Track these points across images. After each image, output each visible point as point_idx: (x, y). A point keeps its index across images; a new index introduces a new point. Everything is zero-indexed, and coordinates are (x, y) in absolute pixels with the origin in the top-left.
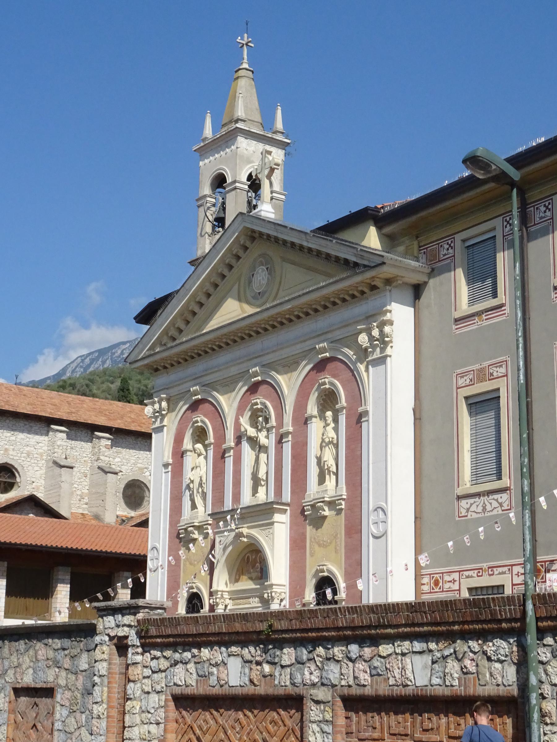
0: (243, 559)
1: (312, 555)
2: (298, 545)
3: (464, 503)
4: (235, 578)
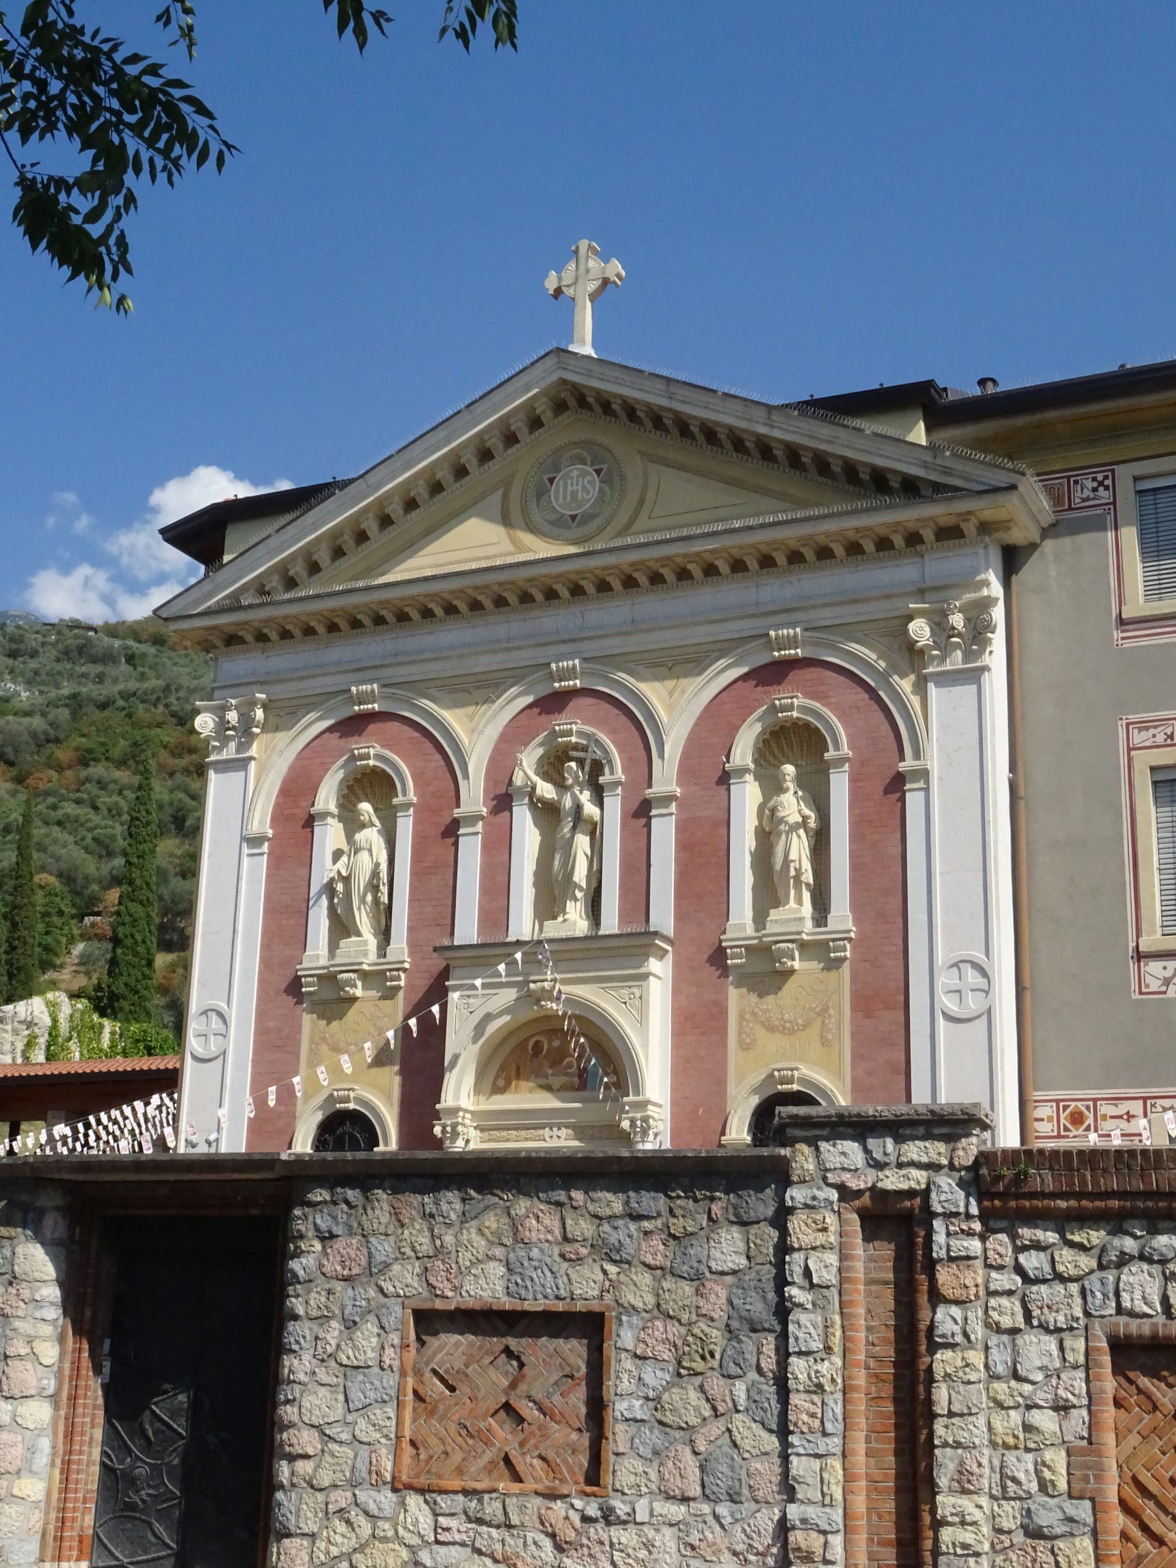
0: (521, 1046)
1: (745, 1047)
2: (699, 1028)
3: (1155, 968)
4: (494, 1084)
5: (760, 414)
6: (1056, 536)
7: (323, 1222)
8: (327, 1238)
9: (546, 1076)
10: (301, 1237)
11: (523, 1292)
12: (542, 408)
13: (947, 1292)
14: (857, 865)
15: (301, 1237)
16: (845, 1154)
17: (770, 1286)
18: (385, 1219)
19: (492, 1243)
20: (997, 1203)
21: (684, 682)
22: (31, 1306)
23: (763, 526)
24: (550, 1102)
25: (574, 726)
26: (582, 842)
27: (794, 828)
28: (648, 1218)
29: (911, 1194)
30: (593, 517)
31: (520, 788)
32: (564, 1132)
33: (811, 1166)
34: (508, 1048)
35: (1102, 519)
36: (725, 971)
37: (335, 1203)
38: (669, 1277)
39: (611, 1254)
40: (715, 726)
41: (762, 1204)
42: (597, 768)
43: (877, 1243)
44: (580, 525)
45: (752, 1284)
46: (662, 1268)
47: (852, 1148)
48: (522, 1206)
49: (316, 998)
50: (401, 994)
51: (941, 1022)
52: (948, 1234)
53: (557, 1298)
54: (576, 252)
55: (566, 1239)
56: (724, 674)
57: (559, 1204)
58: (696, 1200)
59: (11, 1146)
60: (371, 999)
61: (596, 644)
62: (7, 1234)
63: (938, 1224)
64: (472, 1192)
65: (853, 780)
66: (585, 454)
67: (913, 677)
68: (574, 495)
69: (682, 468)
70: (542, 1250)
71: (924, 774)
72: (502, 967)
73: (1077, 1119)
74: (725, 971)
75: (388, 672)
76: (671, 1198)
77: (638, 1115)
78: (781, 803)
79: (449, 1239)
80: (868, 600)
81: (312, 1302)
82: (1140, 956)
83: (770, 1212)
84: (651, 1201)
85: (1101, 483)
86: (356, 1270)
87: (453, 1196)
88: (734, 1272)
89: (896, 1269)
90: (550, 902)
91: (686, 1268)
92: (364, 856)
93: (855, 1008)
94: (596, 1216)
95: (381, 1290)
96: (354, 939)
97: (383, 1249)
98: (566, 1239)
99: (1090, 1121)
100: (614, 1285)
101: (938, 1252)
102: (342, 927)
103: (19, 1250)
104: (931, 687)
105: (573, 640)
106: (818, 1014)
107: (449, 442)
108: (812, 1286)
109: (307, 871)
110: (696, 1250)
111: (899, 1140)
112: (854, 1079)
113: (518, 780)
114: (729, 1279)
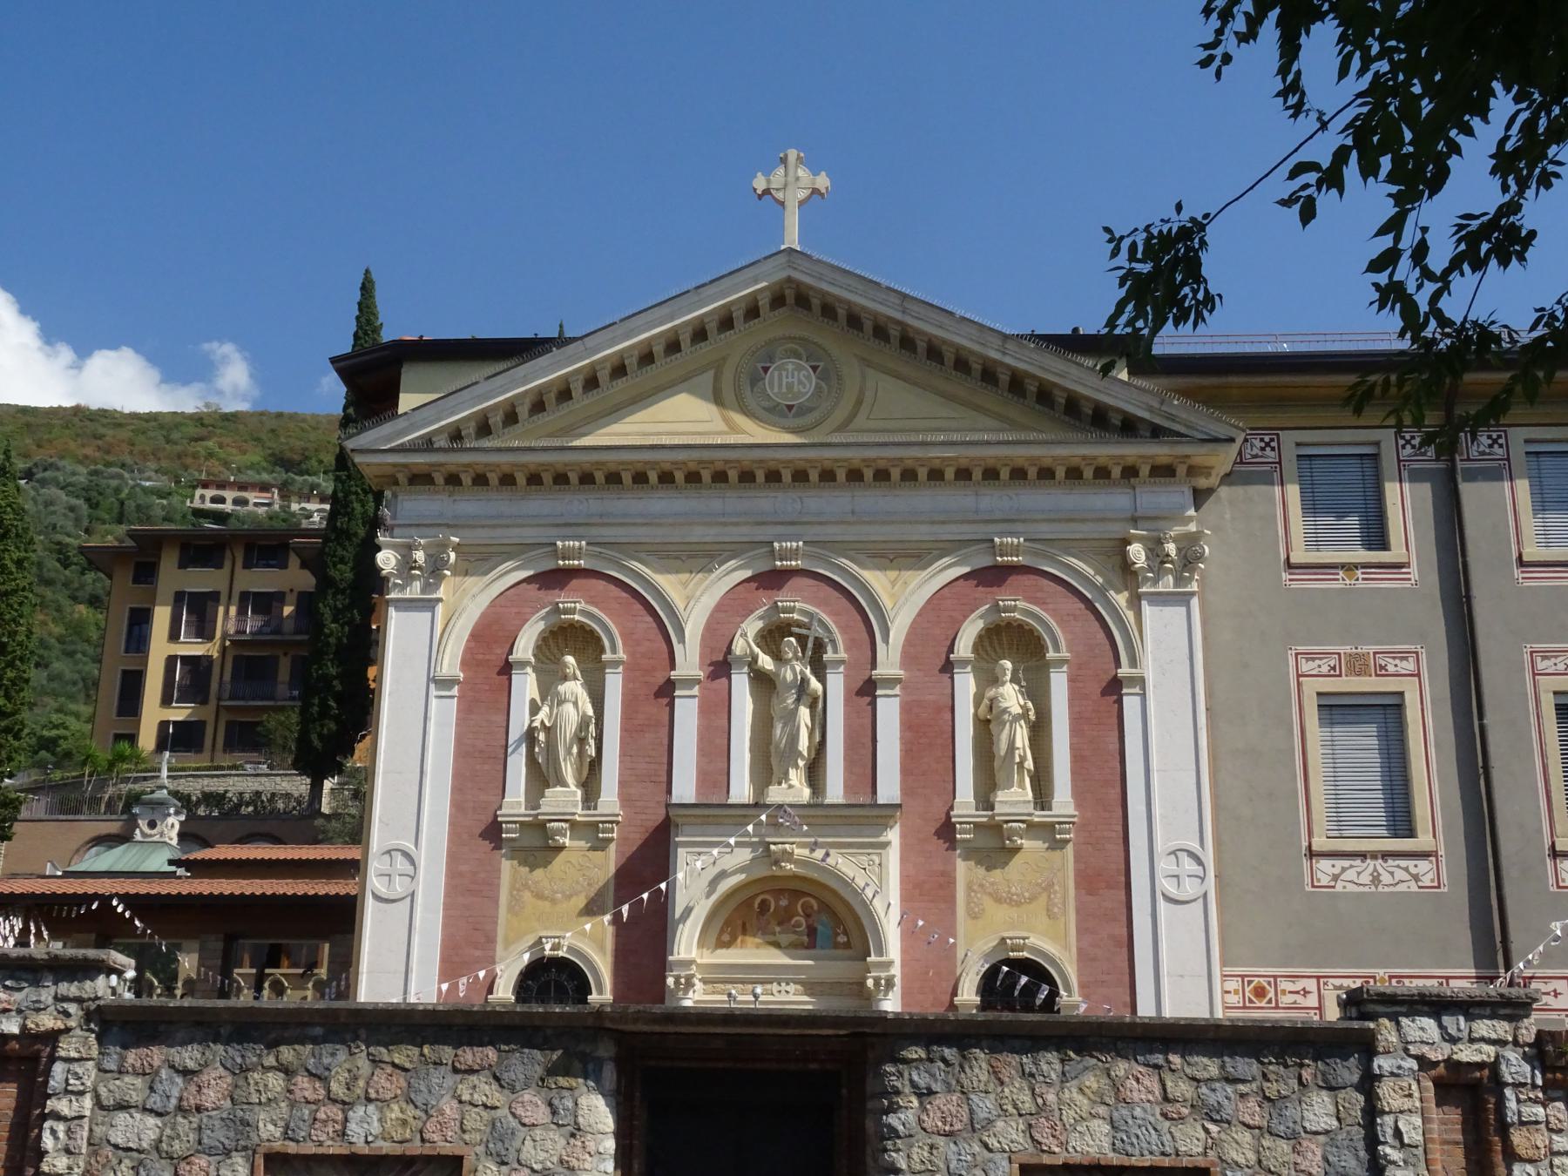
0: (748, 903)
1: (973, 916)
2: (929, 894)
3: (1324, 865)
4: (718, 939)
5: (997, 342)
6: (1231, 484)
7: (922, 1080)
8: (925, 1094)
9: (774, 934)
10: (898, 1093)
11: (1129, 1149)
12: (764, 302)
13: (1522, 1152)
14: (1078, 758)
15: (898, 1093)
16: (1423, 1028)
17: (1361, 1145)
18: (984, 1078)
19: (1094, 1102)
20: (1559, 1075)
21: (907, 574)
22: (595, 1159)
23: (999, 443)
24: (778, 958)
25: (796, 603)
26: (804, 713)
27: (1016, 718)
28: (1243, 1081)
29: (1481, 1066)
30: (811, 410)
31: (739, 658)
32: (792, 988)
33: (1394, 1038)
34: (732, 904)
35: (1271, 475)
36: (952, 843)
37: (931, 1061)
38: (1267, 1136)
39: (1211, 1114)
40: (938, 618)
41: (1348, 1071)
42: (819, 647)
43: (1446, 1108)
44: (797, 415)
45: (1346, 1143)
46: (1259, 1128)
47: (1429, 1023)
48: (1121, 1067)
49: (517, 844)
50: (613, 846)
51: (1162, 905)
52: (1519, 1101)
53: (1163, 1154)
54: (784, 161)
55: (1166, 1099)
56: (946, 571)
57: (1157, 1067)
58: (1286, 1066)
59: (223, 982)
60: (580, 849)
61: (817, 529)
62: (566, 1084)
63: (1509, 1092)
64: (1071, 1054)
65: (1072, 680)
66: (801, 350)
67: (1126, 594)
68: (790, 386)
69: (898, 376)
70: (1145, 1111)
71: (1141, 681)
72: (750, 828)
73: (1260, 992)
74: (952, 843)
75: (594, 531)
76: (1262, 1063)
77: (883, 975)
78: (1002, 695)
79: (1051, 1097)
80: (1083, 521)
81: (915, 1157)
82: (1312, 854)
83: (1355, 1078)
84: (1245, 1066)
85: (1268, 444)
86: (958, 1126)
87: (1052, 1056)
88: (1327, 1132)
89: (1464, 1132)
90: (767, 769)
91: (1282, 1128)
92: (569, 708)
93: (1078, 886)
94: (1194, 1079)
95: (986, 1146)
96: (559, 789)
97: (985, 1106)
98: (1166, 1099)
99: (1271, 995)
100: (1216, 1144)
101: (1511, 1117)
102: (542, 776)
103: (583, 1101)
104: (1144, 603)
105: (792, 523)
106: (1044, 889)
107: (672, 319)
108: (1403, 1145)
109: (501, 718)
110: (1291, 1112)
111: (1470, 1018)
112: (1080, 951)
113: (739, 647)
114: (1322, 1138)
